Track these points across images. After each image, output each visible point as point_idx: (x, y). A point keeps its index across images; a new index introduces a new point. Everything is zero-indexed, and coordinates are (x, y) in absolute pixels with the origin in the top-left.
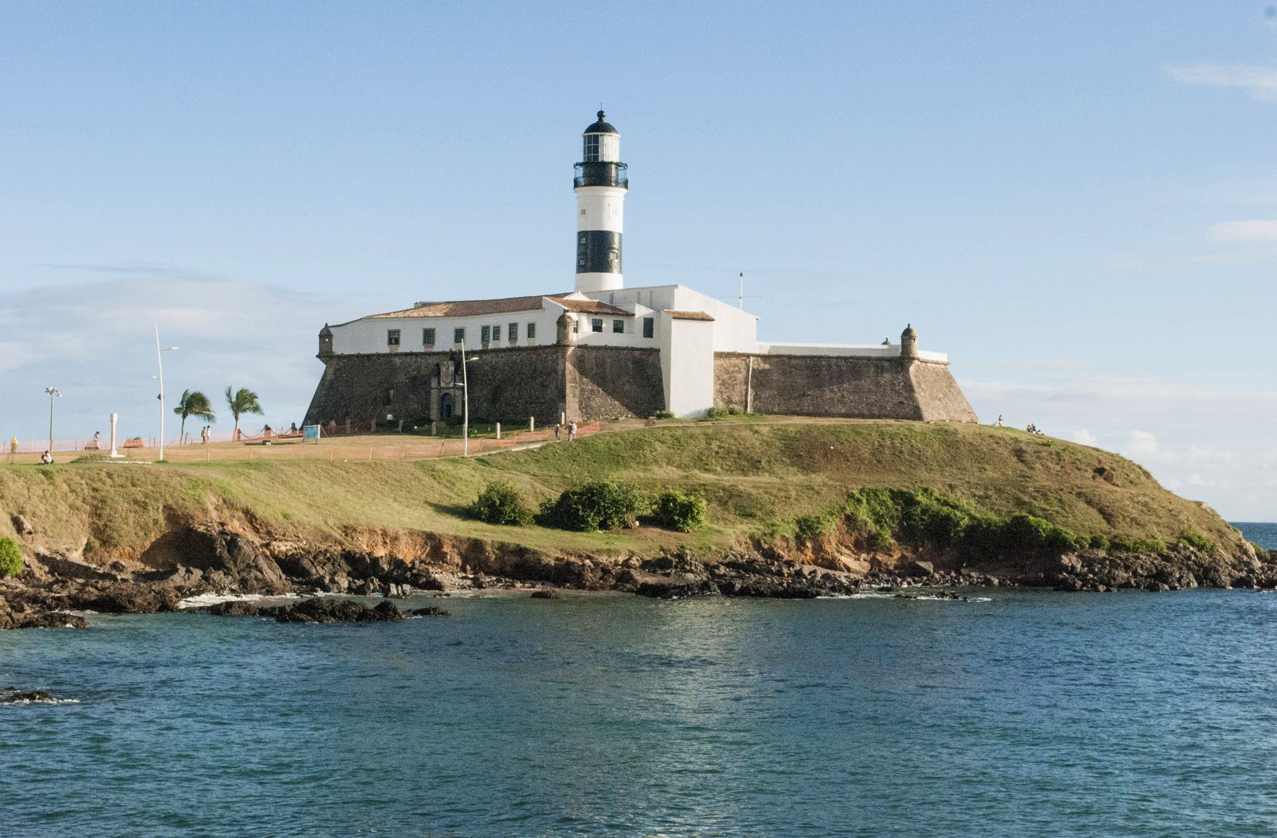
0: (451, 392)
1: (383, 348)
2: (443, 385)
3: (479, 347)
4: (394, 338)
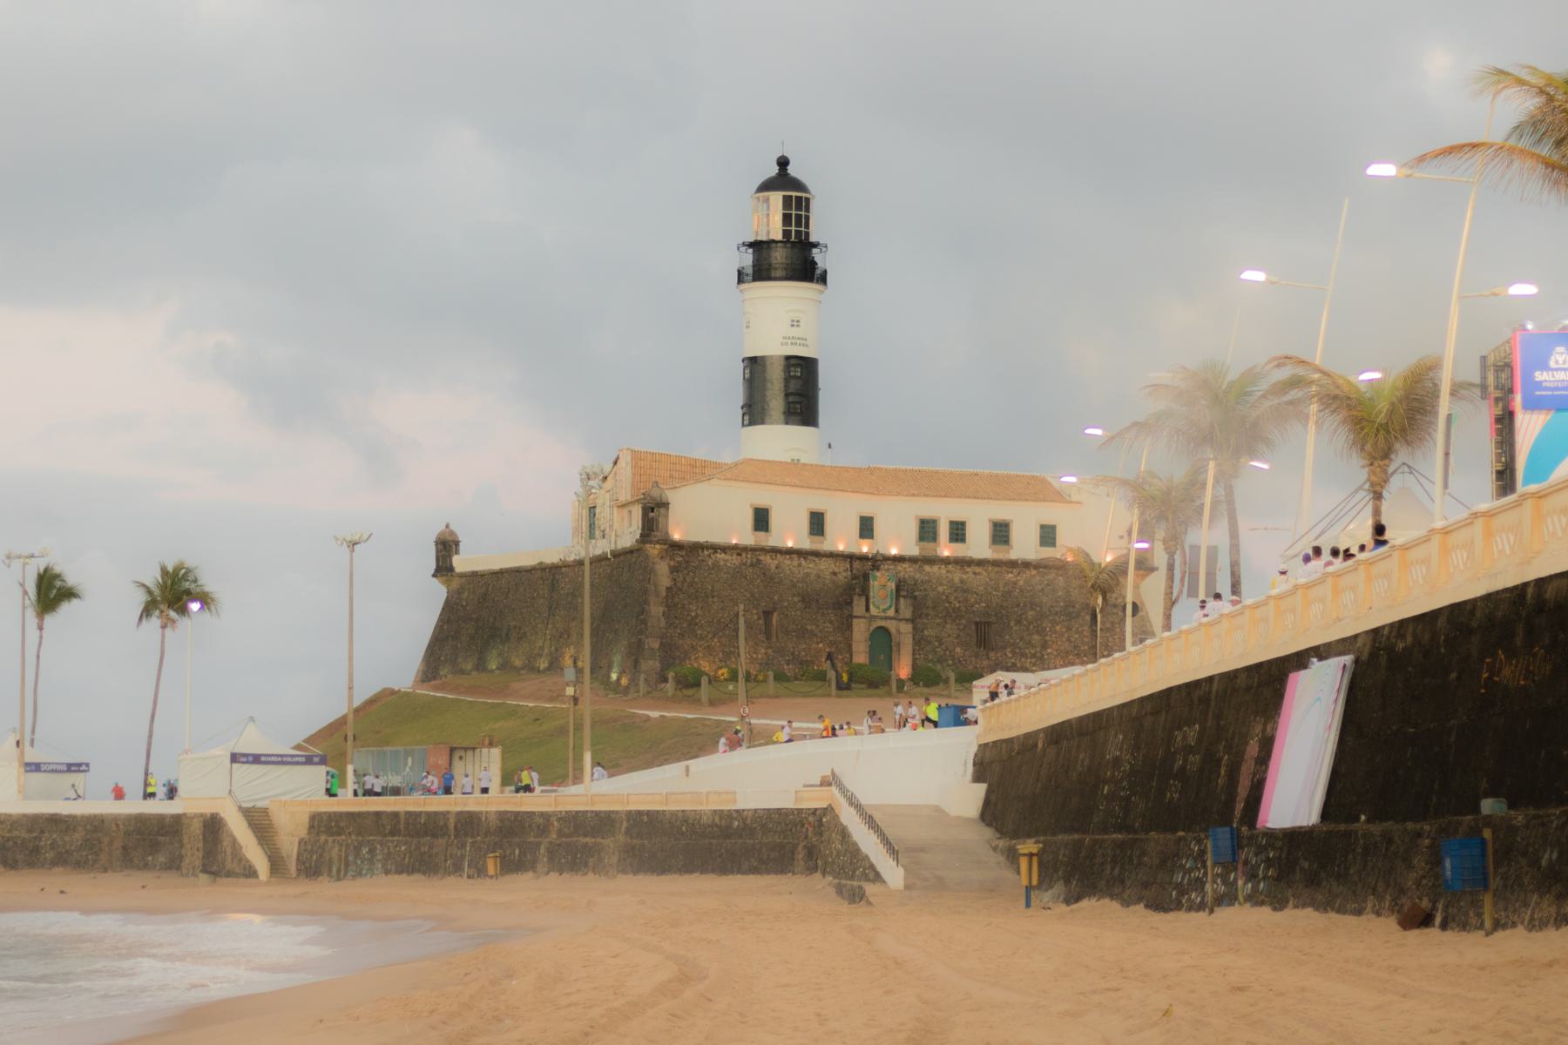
0: (891, 626)
1: (741, 533)
2: (873, 611)
3: (914, 550)
4: (761, 519)
